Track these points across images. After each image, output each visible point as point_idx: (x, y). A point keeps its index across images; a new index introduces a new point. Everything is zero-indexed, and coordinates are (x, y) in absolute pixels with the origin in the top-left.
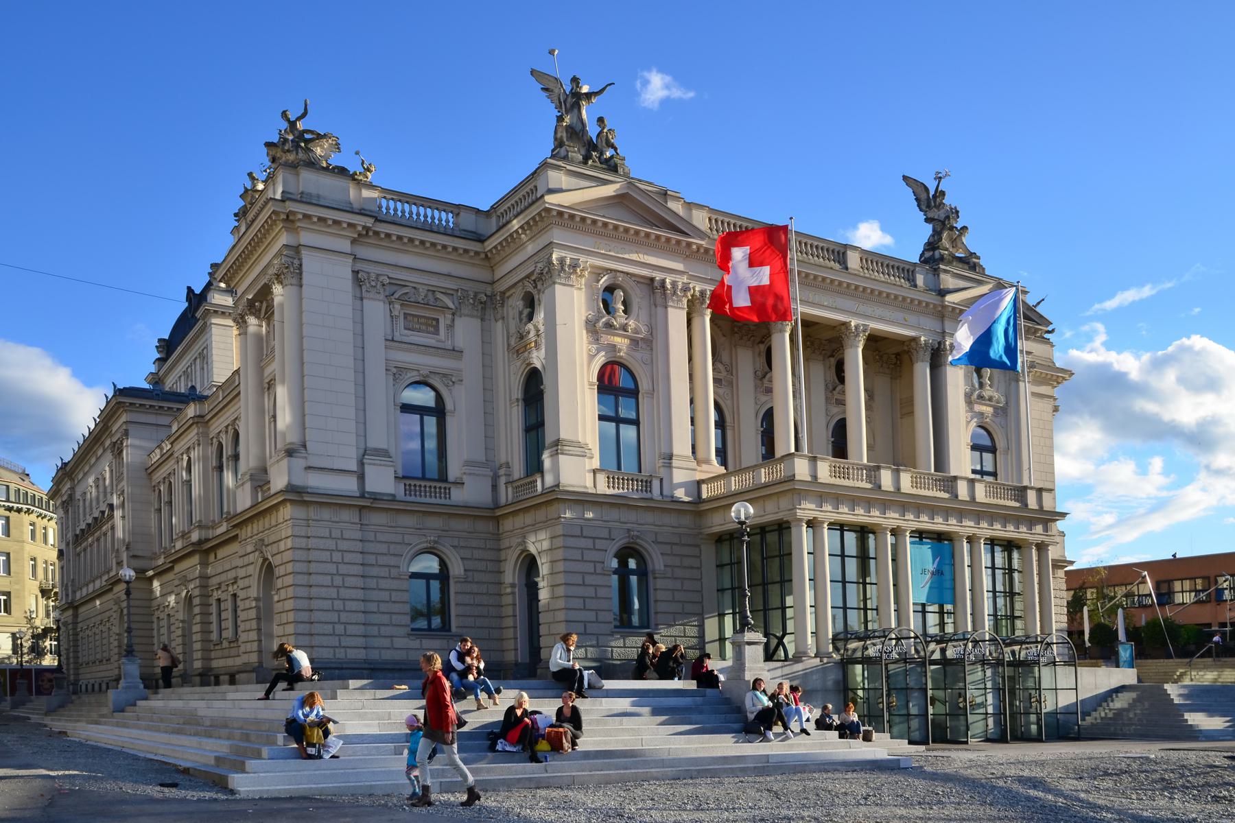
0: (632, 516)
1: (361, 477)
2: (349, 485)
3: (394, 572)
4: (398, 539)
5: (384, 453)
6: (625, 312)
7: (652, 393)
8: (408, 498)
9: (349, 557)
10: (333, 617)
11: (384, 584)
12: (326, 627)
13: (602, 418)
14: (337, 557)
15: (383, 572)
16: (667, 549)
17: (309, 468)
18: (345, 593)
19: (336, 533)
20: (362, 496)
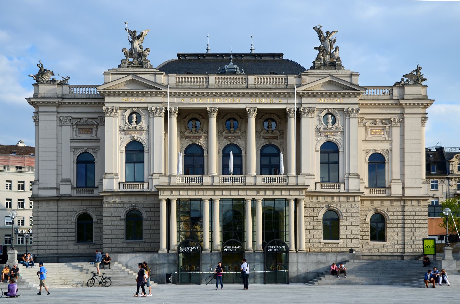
0: (133, 199)
1: (58, 189)
2: (53, 193)
3: (69, 222)
4: (72, 210)
5: (69, 180)
6: (136, 122)
7: (148, 151)
9: (52, 218)
10: (46, 239)
11: (65, 226)
12: (43, 242)
14: (48, 218)
16: (149, 210)
18: (50, 231)
19: (48, 210)
20: (57, 197)
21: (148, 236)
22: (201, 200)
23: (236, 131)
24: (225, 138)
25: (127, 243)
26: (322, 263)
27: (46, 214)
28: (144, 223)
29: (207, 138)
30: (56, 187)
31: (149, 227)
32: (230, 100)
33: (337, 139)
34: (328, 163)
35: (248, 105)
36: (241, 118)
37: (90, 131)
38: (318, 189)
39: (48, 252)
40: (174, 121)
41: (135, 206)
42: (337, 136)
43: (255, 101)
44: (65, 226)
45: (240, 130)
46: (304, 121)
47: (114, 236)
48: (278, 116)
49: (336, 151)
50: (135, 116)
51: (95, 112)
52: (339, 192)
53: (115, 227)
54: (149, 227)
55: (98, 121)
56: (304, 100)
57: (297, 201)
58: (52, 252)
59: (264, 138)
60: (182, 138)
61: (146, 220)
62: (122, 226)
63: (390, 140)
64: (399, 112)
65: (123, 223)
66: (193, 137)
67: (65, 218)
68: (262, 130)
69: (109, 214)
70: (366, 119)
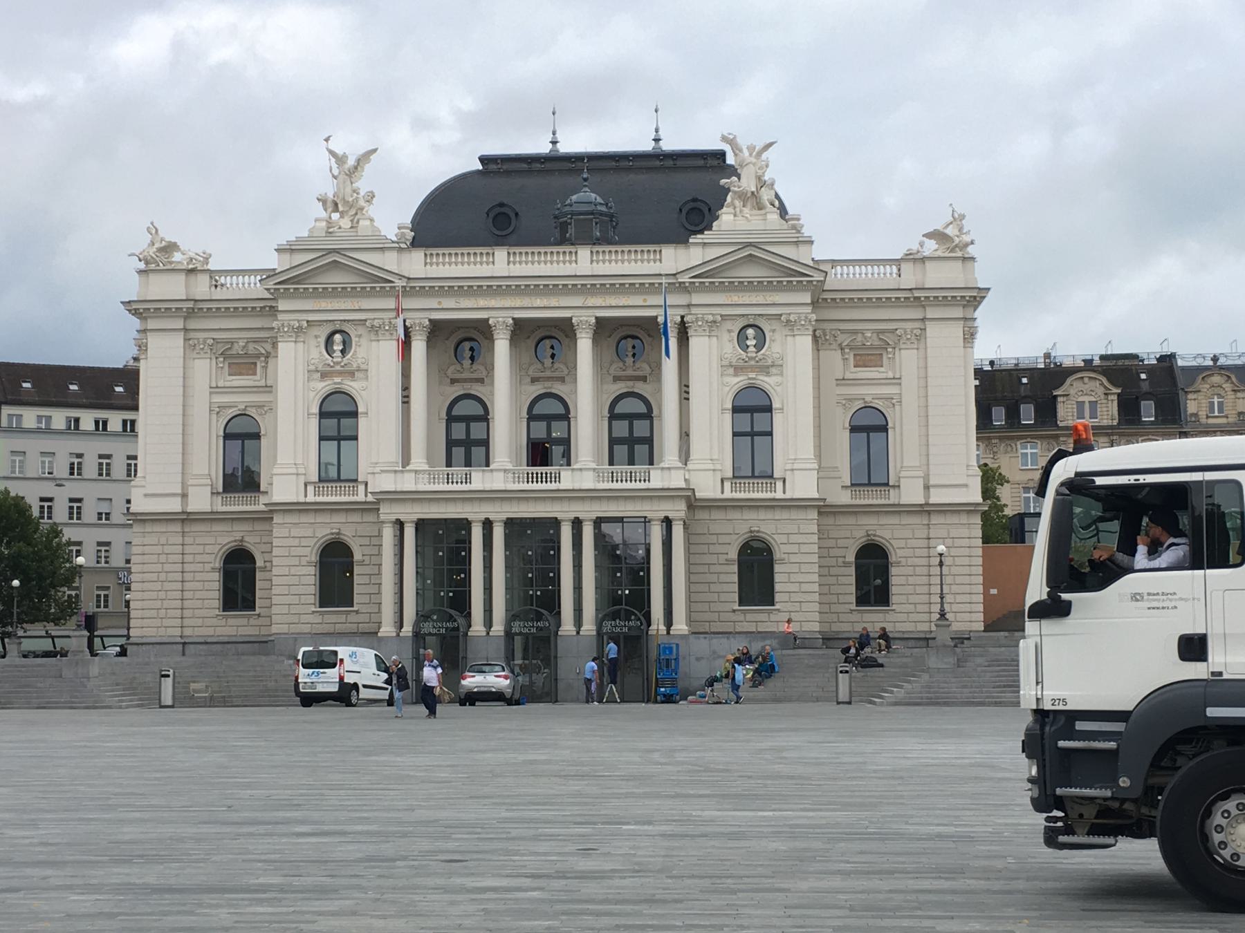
1: (184, 496)
2: (174, 506)
8: (225, 509)
9: (172, 558)
10: (158, 604)
11: (199, 576)
13: (321, 438)
14: (163, 558)
15: (199, 567)
17: (146, 495)
19: (163, 541)
20: (183, 512)
21: (366, 599)
22: (466, 524)
23: (556, 366)
24: (534, 380)
25: (322, 613)
26: (719, 657)
27: (158, 549)
28: (357, 570)
29: (492, 384)
30: (180, 491)
31: (366, 580)
32: (538, 302)
33: (768, 382)
34: (752, 434)
35: (578, 313)
36: (567, 336)
37: (250, 368)
38: (728, 494)
39: (162, 632)
40: (419, 347)
41: (338, 534)
42: (768, 374)
43: (592, 301)
44: (199, 576)
45: (565, 364)
46: (698, 344)
47: (295, 600)
48: (646, 330)
49: (768, 409)
50: (338, 338)
51: (262, 329)
52: (774, 500)
53: (295, 580)
54: (366, 580)
55: (268, 347)
56: (697, 299)
57: (668, 522)
58: (171, 632)
59: (616, 379)
60: (440, 383)
61: (362, 563)
62: (308, 578)
63: (896, 381)
64: (917, 314)
65: (312, 570)
66: (465, 380)
67: (198, 558)
68: (612, 363)
69: (284, 552)
70: (843, 332)
